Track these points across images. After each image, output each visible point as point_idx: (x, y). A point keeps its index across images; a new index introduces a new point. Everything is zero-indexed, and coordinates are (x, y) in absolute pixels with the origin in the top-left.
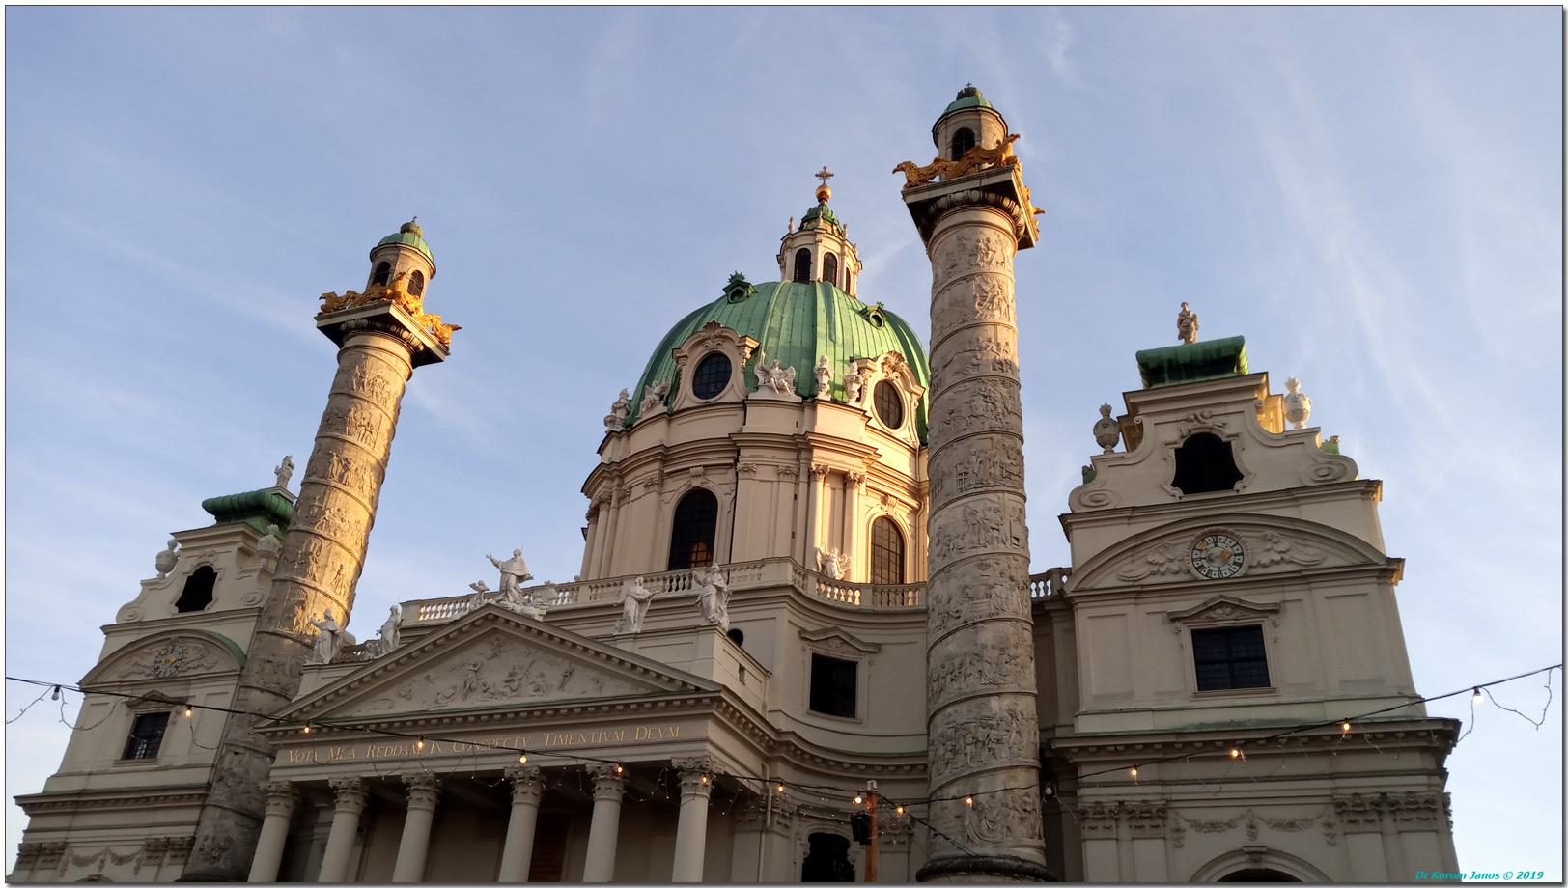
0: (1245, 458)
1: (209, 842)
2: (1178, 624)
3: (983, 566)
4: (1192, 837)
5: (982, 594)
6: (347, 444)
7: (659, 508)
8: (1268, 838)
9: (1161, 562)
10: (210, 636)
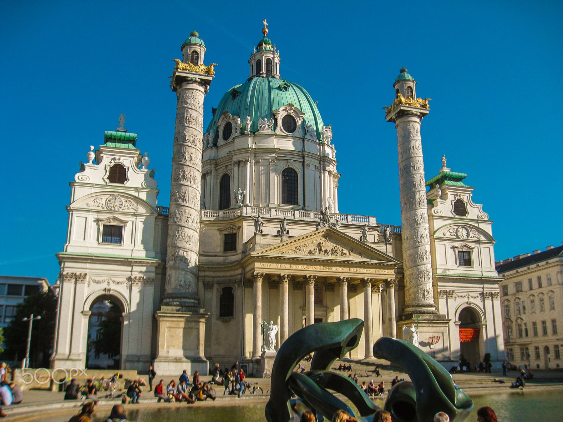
0: (469, 208)
1: (182, 283)
2: (456, 249)
5: (426, 237)
8: (471, 300)
9: (452, 232)
10: (135, 197)
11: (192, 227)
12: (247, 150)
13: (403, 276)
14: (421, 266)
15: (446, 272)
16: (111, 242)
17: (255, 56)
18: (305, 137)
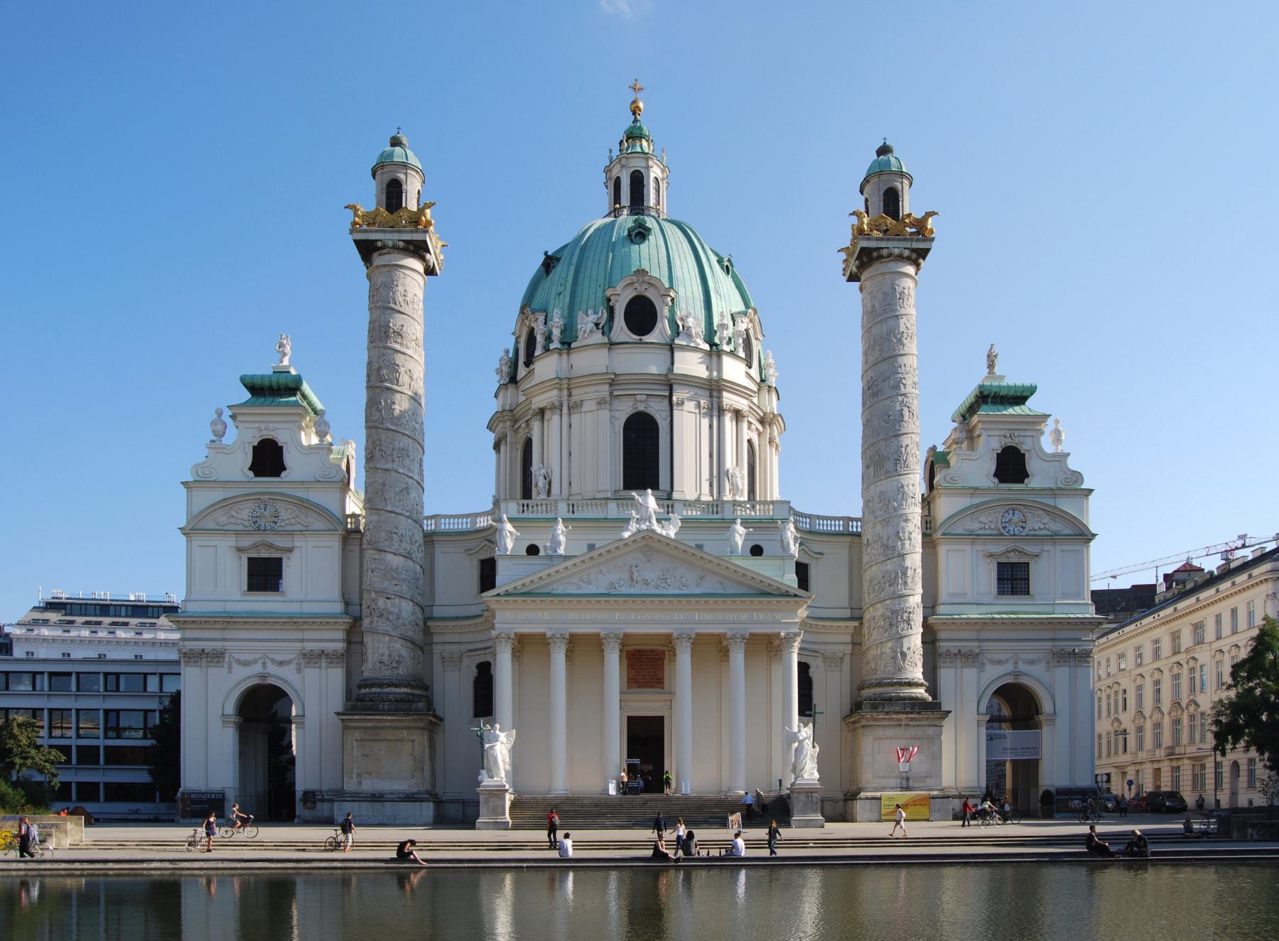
1: (385, 658)
7: (611, 420)
9: (986, 522)
13: (861, 624)
16: (266, 591)
18: (677, 341)
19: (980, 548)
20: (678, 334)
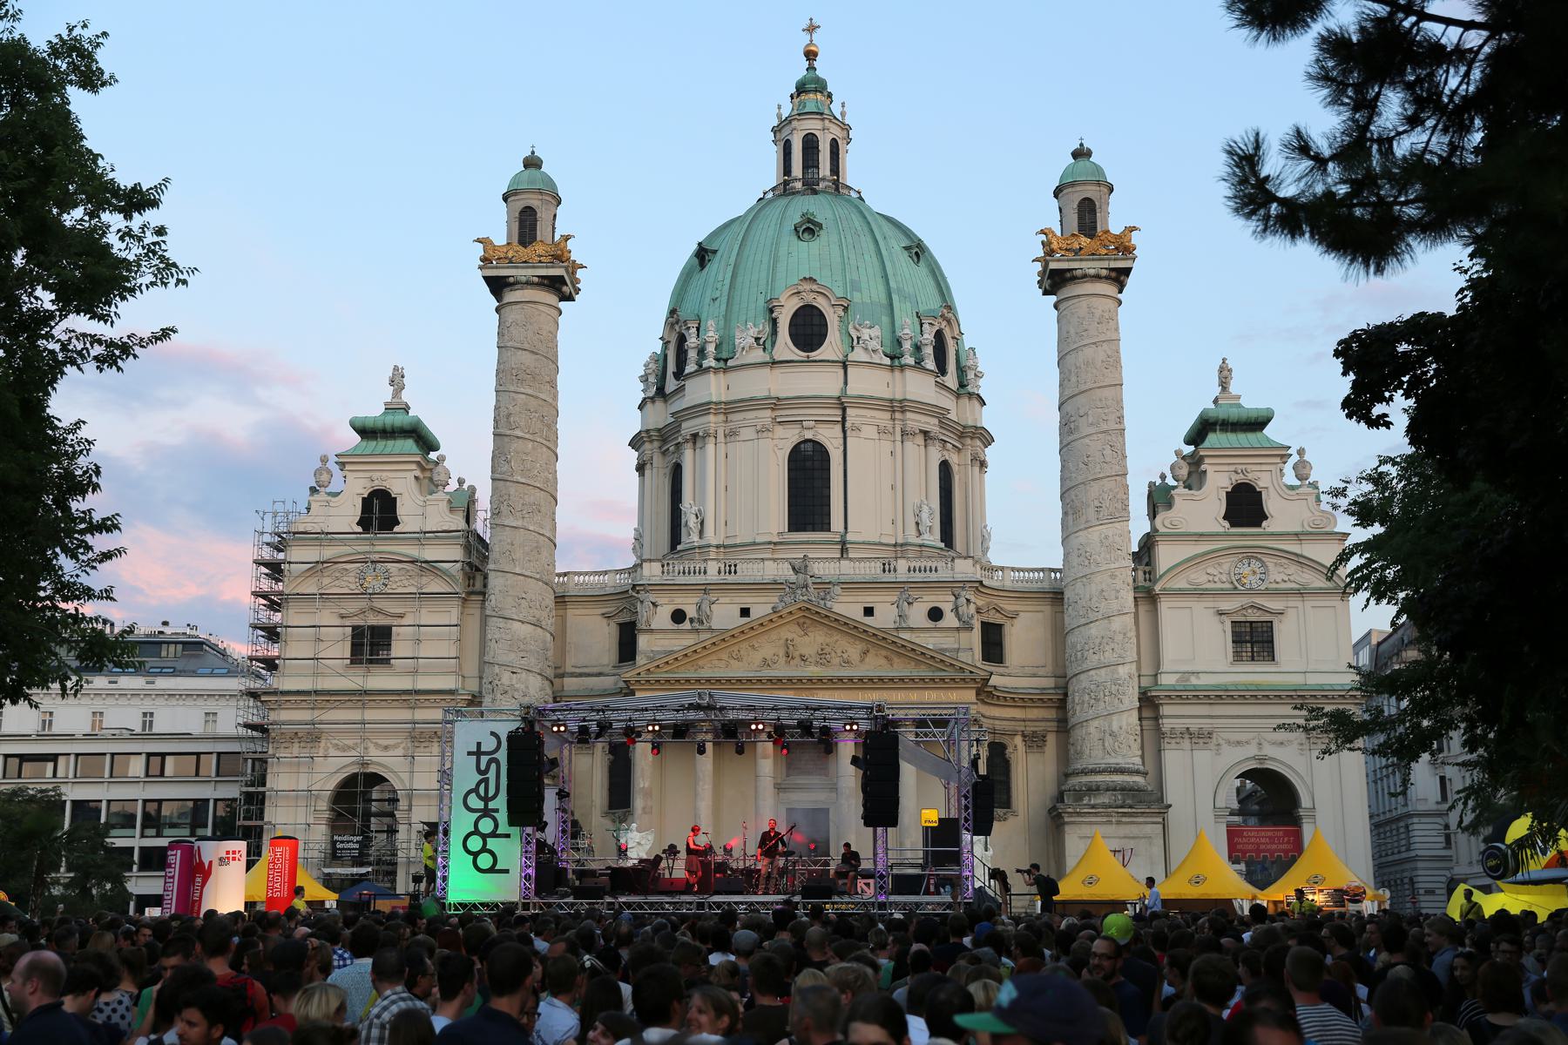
0: (1271, 504)
3: (1113, 576)
4: (1225, 746)
5: (1113, 597)
6: (541, 402)
8: (1269, 751)
11: (530, 619)
12: (703, 409)
13: (1066, 695)
14: (1097, 671)
15: (1188, 680)
17: (780, 131)
19: (1211, 604)
20: (853, 348)
